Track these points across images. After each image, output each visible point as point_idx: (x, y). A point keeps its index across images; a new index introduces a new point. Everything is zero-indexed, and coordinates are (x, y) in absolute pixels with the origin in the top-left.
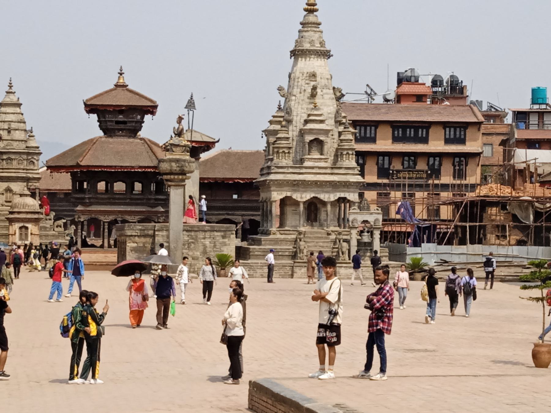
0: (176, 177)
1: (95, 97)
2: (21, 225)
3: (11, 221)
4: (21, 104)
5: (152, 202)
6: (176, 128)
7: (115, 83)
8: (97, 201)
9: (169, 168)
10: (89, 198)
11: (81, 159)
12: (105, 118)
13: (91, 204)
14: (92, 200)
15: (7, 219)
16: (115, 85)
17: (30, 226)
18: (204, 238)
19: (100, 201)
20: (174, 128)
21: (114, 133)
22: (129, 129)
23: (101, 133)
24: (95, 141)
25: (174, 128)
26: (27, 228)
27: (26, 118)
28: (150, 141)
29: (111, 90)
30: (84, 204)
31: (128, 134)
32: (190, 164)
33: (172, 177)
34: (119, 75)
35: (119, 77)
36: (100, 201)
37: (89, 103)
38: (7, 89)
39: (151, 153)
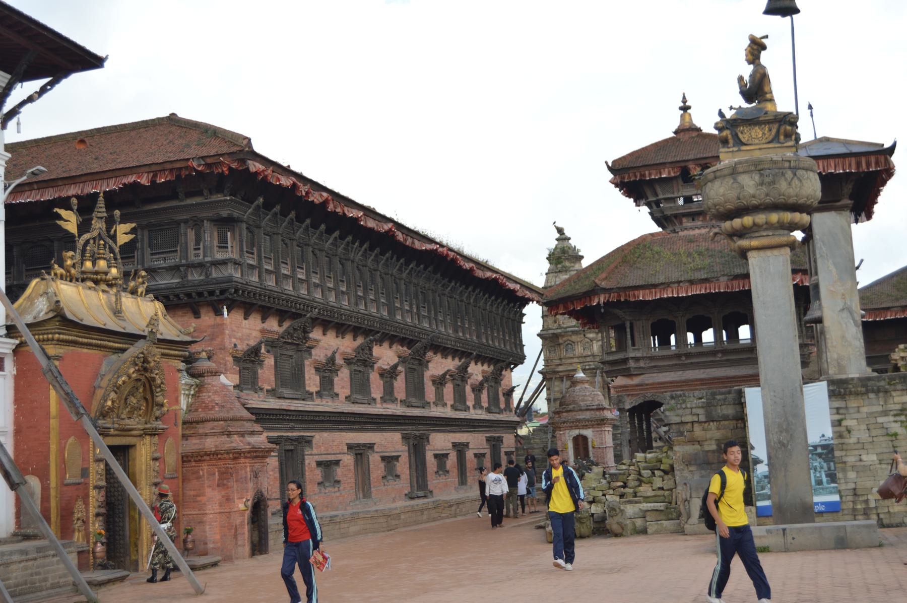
0: (761, 218)
2: (576, 432)
6: (747, 78)
8: (653, 364)
9: (732, 195)
10: (637, 359)
12: (657, 195)
13: (641, 372)
14: (642, 364)
17: (588, 433)
18: (885, 413)
20: (741, 79)
21: (681, 223)
25: (741, 79)
26: (585, 438)
29: (666, 141)
30: (628, 374)
32: (800, 173)
33: (748, 220)
34: (682, 112)
35: (682, 116)
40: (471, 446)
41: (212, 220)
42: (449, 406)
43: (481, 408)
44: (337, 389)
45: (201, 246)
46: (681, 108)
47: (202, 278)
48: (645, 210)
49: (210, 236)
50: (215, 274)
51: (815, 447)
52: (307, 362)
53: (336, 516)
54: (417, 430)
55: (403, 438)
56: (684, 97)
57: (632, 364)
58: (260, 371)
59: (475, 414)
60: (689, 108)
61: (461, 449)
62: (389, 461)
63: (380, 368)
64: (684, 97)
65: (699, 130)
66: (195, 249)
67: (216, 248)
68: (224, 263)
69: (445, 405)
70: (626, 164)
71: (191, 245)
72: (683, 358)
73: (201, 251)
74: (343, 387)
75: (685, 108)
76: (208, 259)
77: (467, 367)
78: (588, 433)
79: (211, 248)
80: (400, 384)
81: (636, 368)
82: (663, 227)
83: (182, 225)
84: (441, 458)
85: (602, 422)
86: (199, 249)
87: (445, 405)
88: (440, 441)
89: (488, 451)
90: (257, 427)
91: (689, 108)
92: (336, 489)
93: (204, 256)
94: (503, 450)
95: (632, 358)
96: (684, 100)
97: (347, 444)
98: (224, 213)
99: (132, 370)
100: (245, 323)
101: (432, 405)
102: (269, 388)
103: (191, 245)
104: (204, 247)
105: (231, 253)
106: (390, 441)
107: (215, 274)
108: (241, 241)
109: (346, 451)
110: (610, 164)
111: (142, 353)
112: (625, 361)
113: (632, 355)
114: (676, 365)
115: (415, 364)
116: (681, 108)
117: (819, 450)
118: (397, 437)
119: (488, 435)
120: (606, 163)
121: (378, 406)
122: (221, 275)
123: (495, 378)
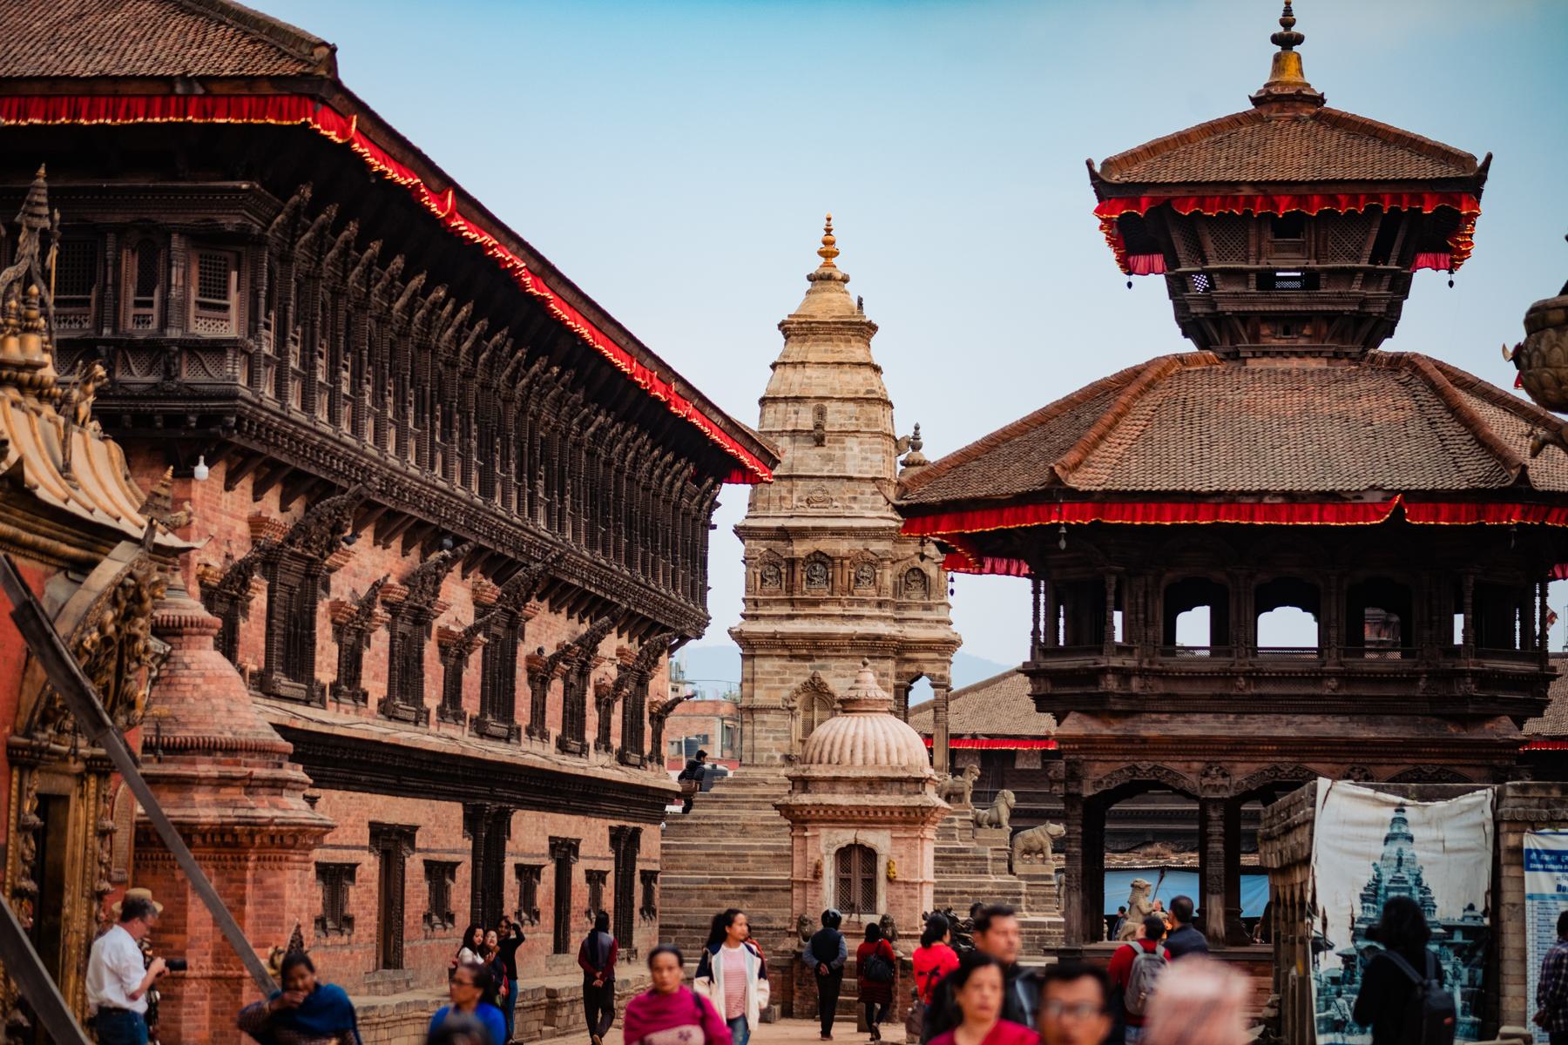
1: (1152, 150)
2: (846, 836)
3: (798, 819)
4: (874, 328)
5: (1460, 689)
7: (1256, 86)
10: (1124, 674)
11: (1071, 457)
15: (786, 810)
16: (1254, 101)
17: (878, 839)
19: (1183, 689)
21: (1255, 337)
22: (1329, 317)
23: (1188, 347)
24: (1149, 376)
26: (870, 855)
27: (891, 384)
28: (1440, 366)
29: (1236, 121)
31: (1333, 346)
34: (1278, 49)
35: (1277, 58)
36: (1183, 689)
37: (1115, 178)
38: (816, 264)
39: (1450, 429)
40: (582, 850)
41: (184, 232)
42: (553, 739)
43: (608, 748)
44: (367, 683)
45: (156, 298)
46: (1276, 39)
47: (151, 379)
48: (1156, 284)
49: (183, 278)
50: (188, 374)
51: (1451, 929)
52: (322, 608)
53: (373, 1008)
54: (489, 793)
55: (466, 816)
56: (1288, 11)
57: (1111, 684)
58: (242, 625)
59: (598, 765)
60: (1299, 39)
61: (564, 851)
62: (439, 872)
63: (444, 632)
64: (1288, 11)
65: (1319, 100)
66: (138, 304)
67: (192, 307)
68: (217, 348)
69: (544, 736)
70: (1137, 174)
71: (130, 293)
72: (1242, 682)
73: (155, 312)
74: (376, 677)
75: (1287, 40)
76: (174, 333)
77: (600, 639)
78: (878, 839)
79: (183, 305)
80: (472, 674)
81: (1122, 696)
82: (1203, 343)
83: (111, 238)
84: (528, 874)
85: (914, 818)
86: (150, 304)
87: (544, 736)
88: (531, 833)
89: (609, 866)
90: (296, 772)
91: (1299, 39)
92: (345, 938)
93: (164, 323)
94: (639, 866)
95: (1115, 670)
96: (1287, 21)
97: (372, 825)
98: (230, 222)
99: (109, 616)
100: (227, 496)
101: (524, 735)
102: (255, 668)
103: (130, 293)
104: (165, 302)
105: (231, 328)
106: (440, 825)
107: (188, 374)
108: (255, 295)
109: (367, 843)
110: (1098, 169)
111: (131, 575)
112: (1096, 675)
113: (1116, 662)
114: (1221, 697)
115: (500, 626)
116: (1276, 39)
117: (1458, 938)
118: (453, 812)
119: (614, 823)
120: (1089, 164)
121: (433, 728)
122: (202, 378)
123: (637, 674)
